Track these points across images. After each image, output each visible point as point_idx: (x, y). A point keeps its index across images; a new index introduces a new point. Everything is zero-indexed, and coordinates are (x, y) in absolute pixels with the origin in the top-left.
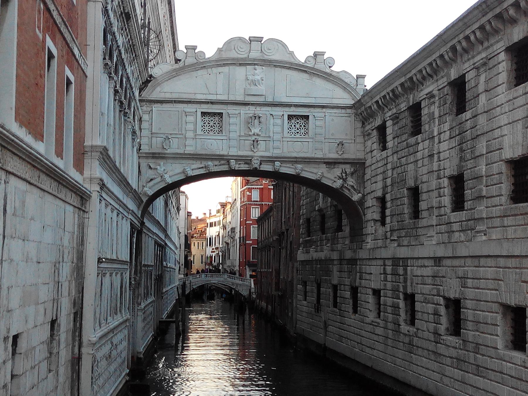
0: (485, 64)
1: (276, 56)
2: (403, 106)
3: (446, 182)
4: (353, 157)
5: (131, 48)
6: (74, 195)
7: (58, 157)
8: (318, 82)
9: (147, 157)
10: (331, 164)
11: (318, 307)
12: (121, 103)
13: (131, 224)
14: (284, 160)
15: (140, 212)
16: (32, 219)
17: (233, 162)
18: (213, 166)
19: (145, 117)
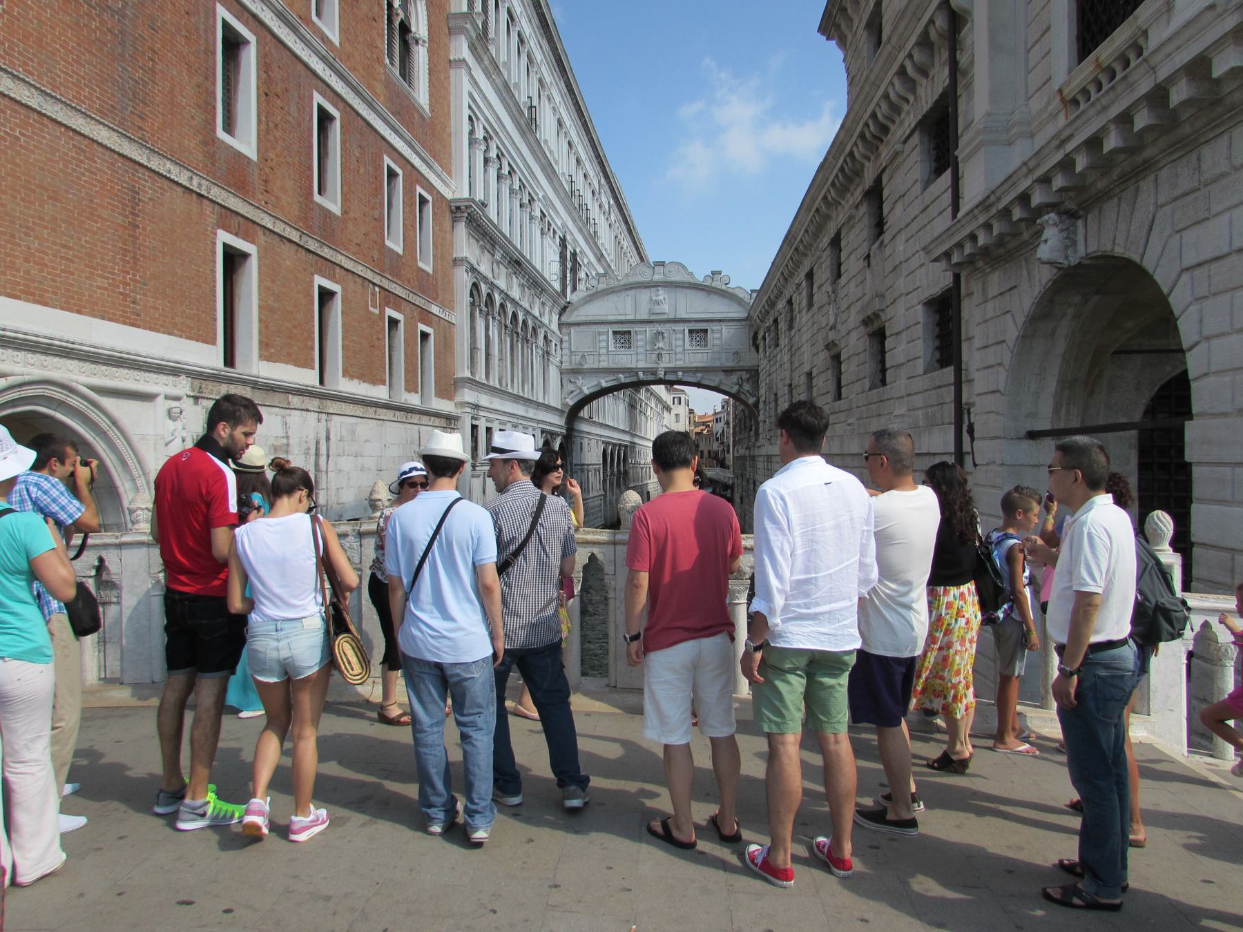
0: (797, 288)
1: (677, 278)
2: (771, 320)
3: (786, 389)
4: (749, 364)
5: (535, 284)
6: (432, 418)
7: (409, 392)
8: (715, 297)
9: (568, 373)
10: (728, 371)
11: (742, 498)
12: (517, 334)
13: (543, 432)
14: (686, 370)
15: (564, 420)
16: (367, 441)
17: (641, 374)
18: (623, 378)
19: (566, 338)
